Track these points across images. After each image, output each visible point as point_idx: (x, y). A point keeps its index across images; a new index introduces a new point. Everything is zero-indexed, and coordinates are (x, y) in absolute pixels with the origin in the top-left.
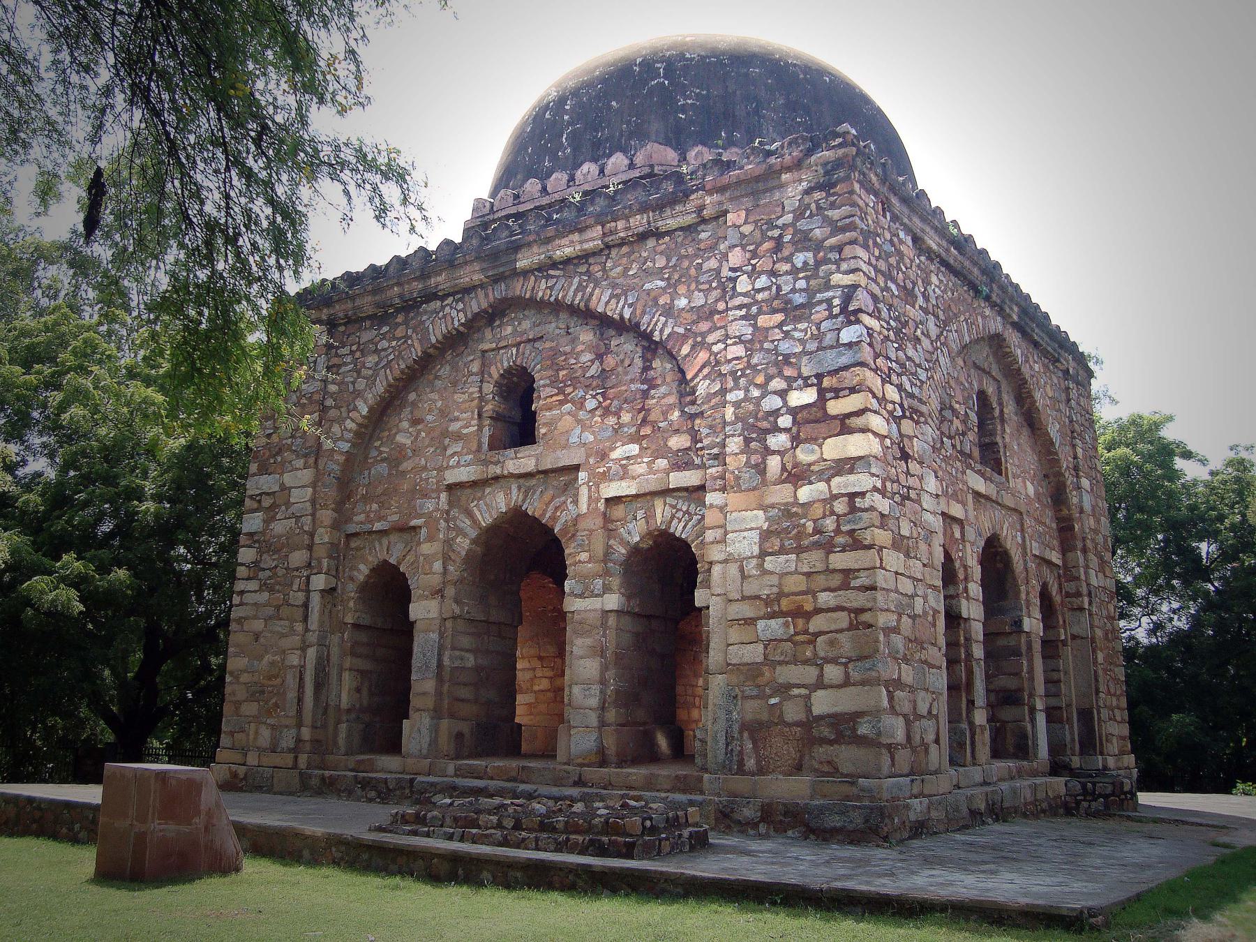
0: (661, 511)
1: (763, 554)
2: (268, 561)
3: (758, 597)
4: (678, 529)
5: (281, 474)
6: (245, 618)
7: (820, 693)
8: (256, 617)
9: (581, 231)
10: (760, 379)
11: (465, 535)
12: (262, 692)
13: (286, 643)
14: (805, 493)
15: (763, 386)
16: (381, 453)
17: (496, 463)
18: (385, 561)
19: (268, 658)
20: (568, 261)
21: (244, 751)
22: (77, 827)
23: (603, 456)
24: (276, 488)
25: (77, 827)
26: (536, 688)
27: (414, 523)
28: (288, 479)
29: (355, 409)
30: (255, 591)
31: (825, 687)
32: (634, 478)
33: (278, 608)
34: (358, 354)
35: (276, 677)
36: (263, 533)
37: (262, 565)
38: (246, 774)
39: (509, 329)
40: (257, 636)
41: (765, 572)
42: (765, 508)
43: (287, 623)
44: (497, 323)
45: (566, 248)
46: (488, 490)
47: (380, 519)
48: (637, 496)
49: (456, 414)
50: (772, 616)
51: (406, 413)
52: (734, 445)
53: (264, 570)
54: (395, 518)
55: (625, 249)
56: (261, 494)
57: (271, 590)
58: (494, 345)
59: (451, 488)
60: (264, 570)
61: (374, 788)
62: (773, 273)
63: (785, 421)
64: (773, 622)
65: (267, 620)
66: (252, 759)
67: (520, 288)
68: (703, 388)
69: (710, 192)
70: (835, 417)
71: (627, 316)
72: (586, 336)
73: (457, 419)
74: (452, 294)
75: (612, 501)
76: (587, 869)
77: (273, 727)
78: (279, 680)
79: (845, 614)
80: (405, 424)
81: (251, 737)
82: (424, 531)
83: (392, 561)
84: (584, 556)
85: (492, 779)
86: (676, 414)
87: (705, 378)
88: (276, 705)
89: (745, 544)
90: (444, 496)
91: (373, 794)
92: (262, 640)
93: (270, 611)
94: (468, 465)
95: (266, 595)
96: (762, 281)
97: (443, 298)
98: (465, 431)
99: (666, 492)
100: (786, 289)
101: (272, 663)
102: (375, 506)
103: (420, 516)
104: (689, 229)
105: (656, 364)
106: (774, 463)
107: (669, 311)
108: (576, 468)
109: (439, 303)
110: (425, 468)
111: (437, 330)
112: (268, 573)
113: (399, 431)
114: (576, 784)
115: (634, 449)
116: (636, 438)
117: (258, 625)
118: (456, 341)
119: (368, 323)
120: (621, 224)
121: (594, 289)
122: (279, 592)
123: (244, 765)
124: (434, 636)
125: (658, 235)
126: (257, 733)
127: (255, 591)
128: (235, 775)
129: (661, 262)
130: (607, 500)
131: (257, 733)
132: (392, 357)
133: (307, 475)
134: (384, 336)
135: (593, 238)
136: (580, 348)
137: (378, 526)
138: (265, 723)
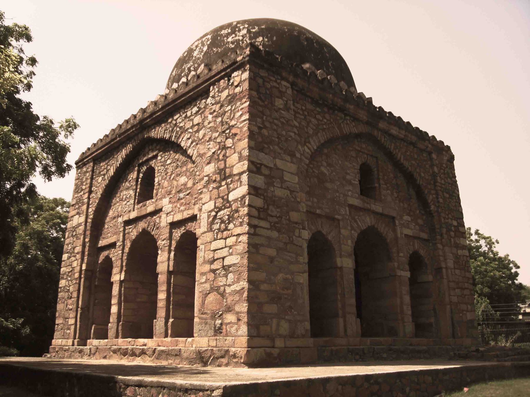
0: (417, 245)
1: (455, 268)
2: (273, 211)
3: (454, 281)
4: (422, 252)
5: (274, 158)
6: (262, 245)
7: (468, 313)
8: (269, 246)
9: (399, 128)
10: (447, 213)
11: (355, 231)
12: (280, 298)
13: (293, 268)
14: (460, 252)
15: (448, 215)
16: (314, 172)
17: (368, 203)
18: (320, 232)
19: (281, 276)
20: (390, 135)
21: (272, 339)
22: (408, 389)
23: (401, 218)
24: (272, 166)
25: (408, 389)
26: (139, 300)
27: (337, 217)
28: (279, 163)
29: (309, 142)
30: (267, 229)
31: (468, 311)
32: (412, 229)
33: (286, 244)
34: (306, 113)
35: (287, 289)
36: (266, 190)
37: (270, 212)
38: (279, 354)
39: (364, 146)
40: (272, 260)
41: (456, 274)
42: (453, 254)
43: (294, 255)
44: (359, 140)
45: (394, 131)
46: (361, 213)
47: (320, 208)
48: (410, 236)
49: (348, 172)
50: (458, 288)
51: (324, 157)
52: (444, 230)
53: (272, 216)
54: (327, 211)
55: (405, 144)
56: (261, 164)
57: (279, 231)
58: (359, 149)
59: (351, 206)
60: (272, 216)
61: (357, 354)
62: (445, 181)
63: (453, 228)
64: (459, 290)
65: (279, 250)
66: (279, 343)
67: (376, 133)
68: (432, 207)
69: (430, 143)
70: (460, 232)
71: (410, 168)
72: (390, 167)
73: (349, 174)
74: (350, 116)
75: (406, 235)
76: (484, 368)
77: (289, 321)
78: (290, 292)
79: (468, 290)
80: (325, 164)
81: (274, 328)
82: (341, 223)
83: (324, 232)
84: (401, 254)
85: (383, 345)
86: (418, 212)
87: (433, 204)
88: (291, 307)
89: (451, 264)
90: (347, 208)
91: (358, 357)
92: (276, 263)
93: (281, 245)
94: (357, 198)
95: (275, 234)
96: (443, 182)
97: (346, 115)
98: (353, 182)
99: (418, 238)
100: (448, 188)
101: (286, 280)
102: (315, 200)
103: (340, 215)
104: (422, 150)
105: (411, 190)
106: (452, 240)
107: (420, 175)
108: (393, 218)
109: (343, 116)
110: (338, 192)
111: (346, 130)
112: (275, 220)
113: (322, 165)
114: (411, 345)
115: (409, 218)
116: (410, 216)
117: (272, 252)
118: (348, 138)
119: (309, 100)
120: (409, 135)
121: (399, 151)
122: (284, 233)
123: (273, 347)
124: (352, 277)
125: (413, 144)
126: (278, 325)
127: (267, 229)
128: (269, 355)
129: (416, 156)
130: (405, 235)
131: (278, 325)
132: (325, 127)
133: (293, 168)
134: (319, 113)
135: (402, 134)
136: (389, 170)
137: (318, 211)
138: (284, 319)
